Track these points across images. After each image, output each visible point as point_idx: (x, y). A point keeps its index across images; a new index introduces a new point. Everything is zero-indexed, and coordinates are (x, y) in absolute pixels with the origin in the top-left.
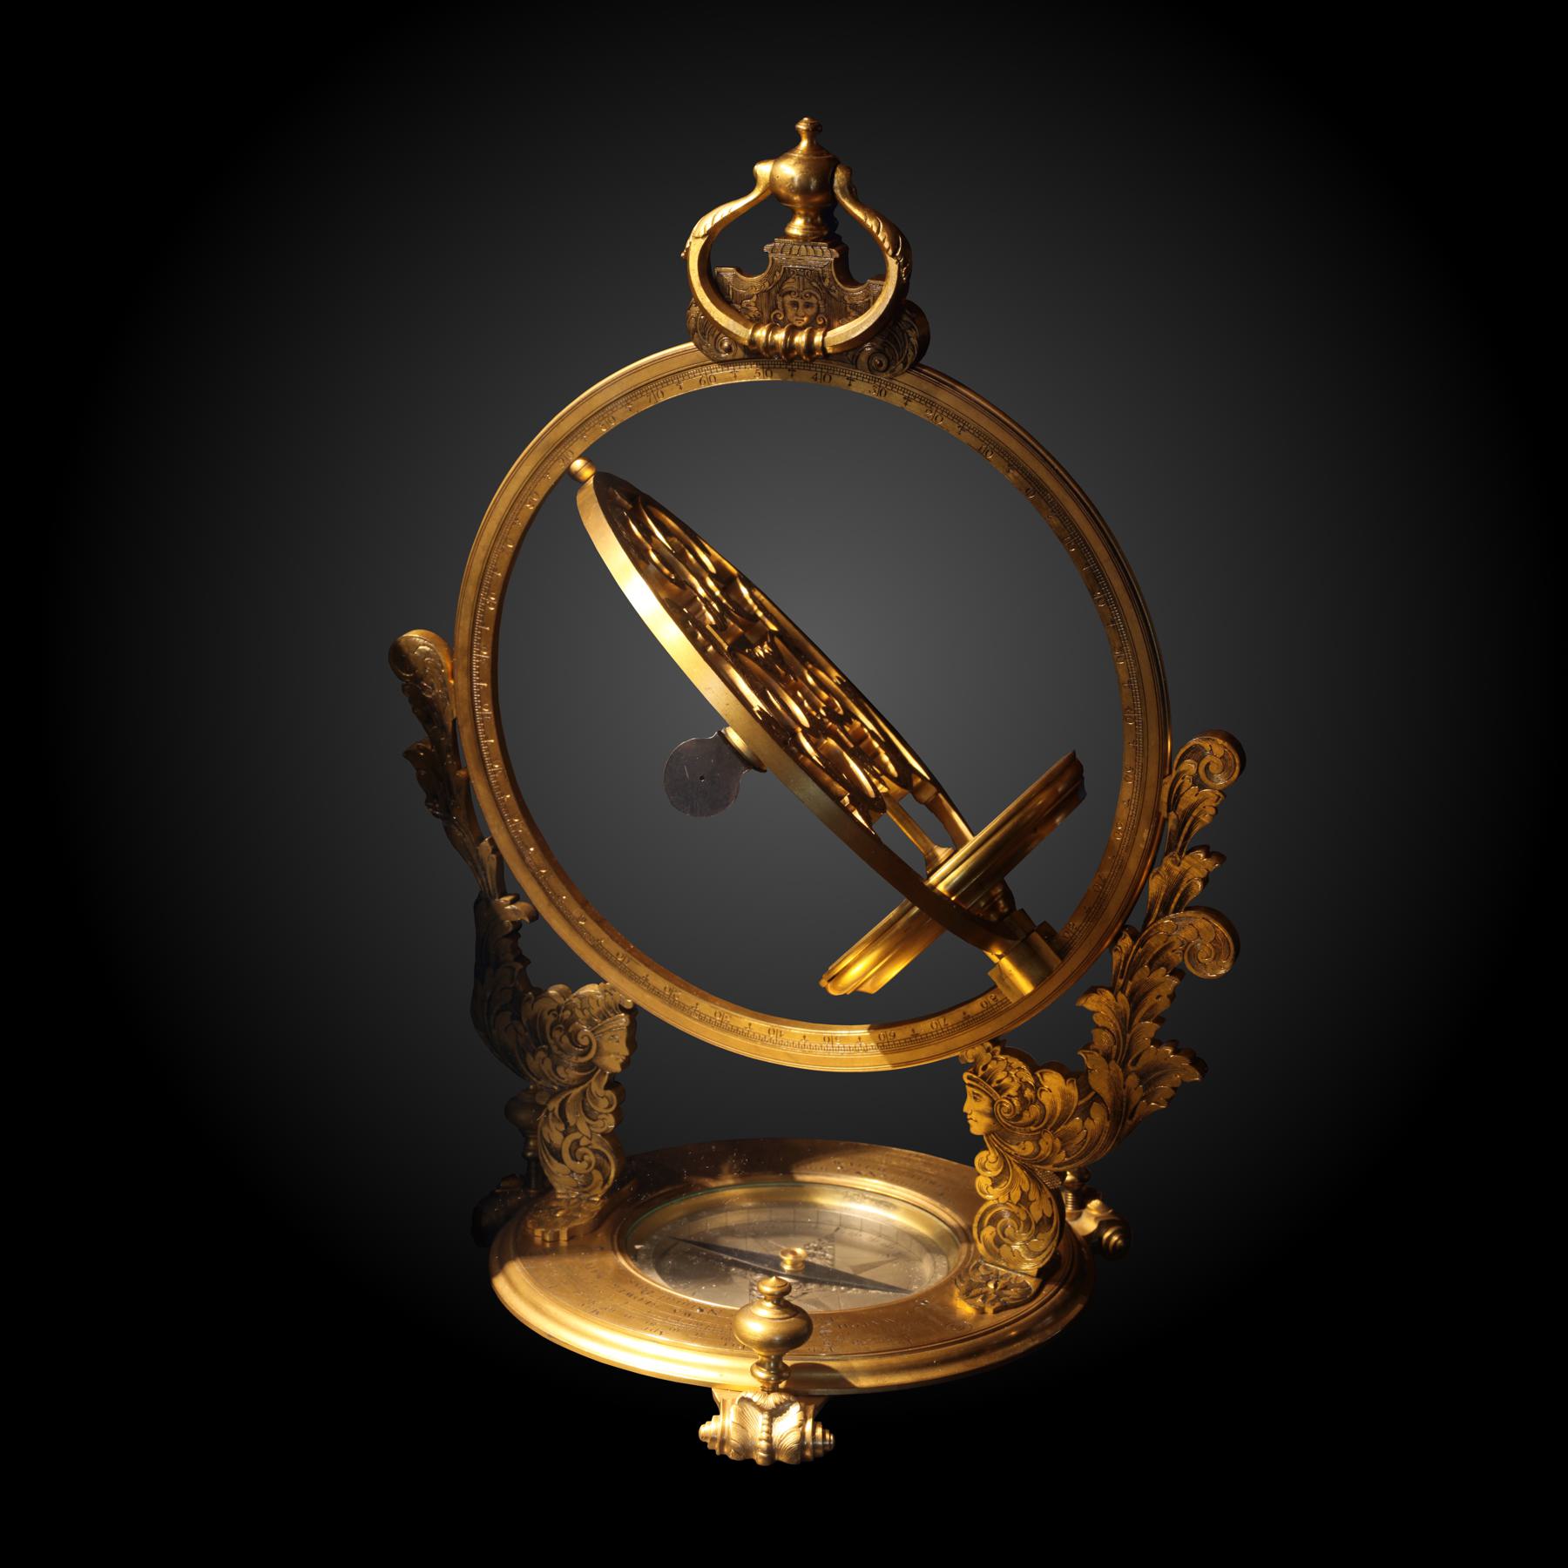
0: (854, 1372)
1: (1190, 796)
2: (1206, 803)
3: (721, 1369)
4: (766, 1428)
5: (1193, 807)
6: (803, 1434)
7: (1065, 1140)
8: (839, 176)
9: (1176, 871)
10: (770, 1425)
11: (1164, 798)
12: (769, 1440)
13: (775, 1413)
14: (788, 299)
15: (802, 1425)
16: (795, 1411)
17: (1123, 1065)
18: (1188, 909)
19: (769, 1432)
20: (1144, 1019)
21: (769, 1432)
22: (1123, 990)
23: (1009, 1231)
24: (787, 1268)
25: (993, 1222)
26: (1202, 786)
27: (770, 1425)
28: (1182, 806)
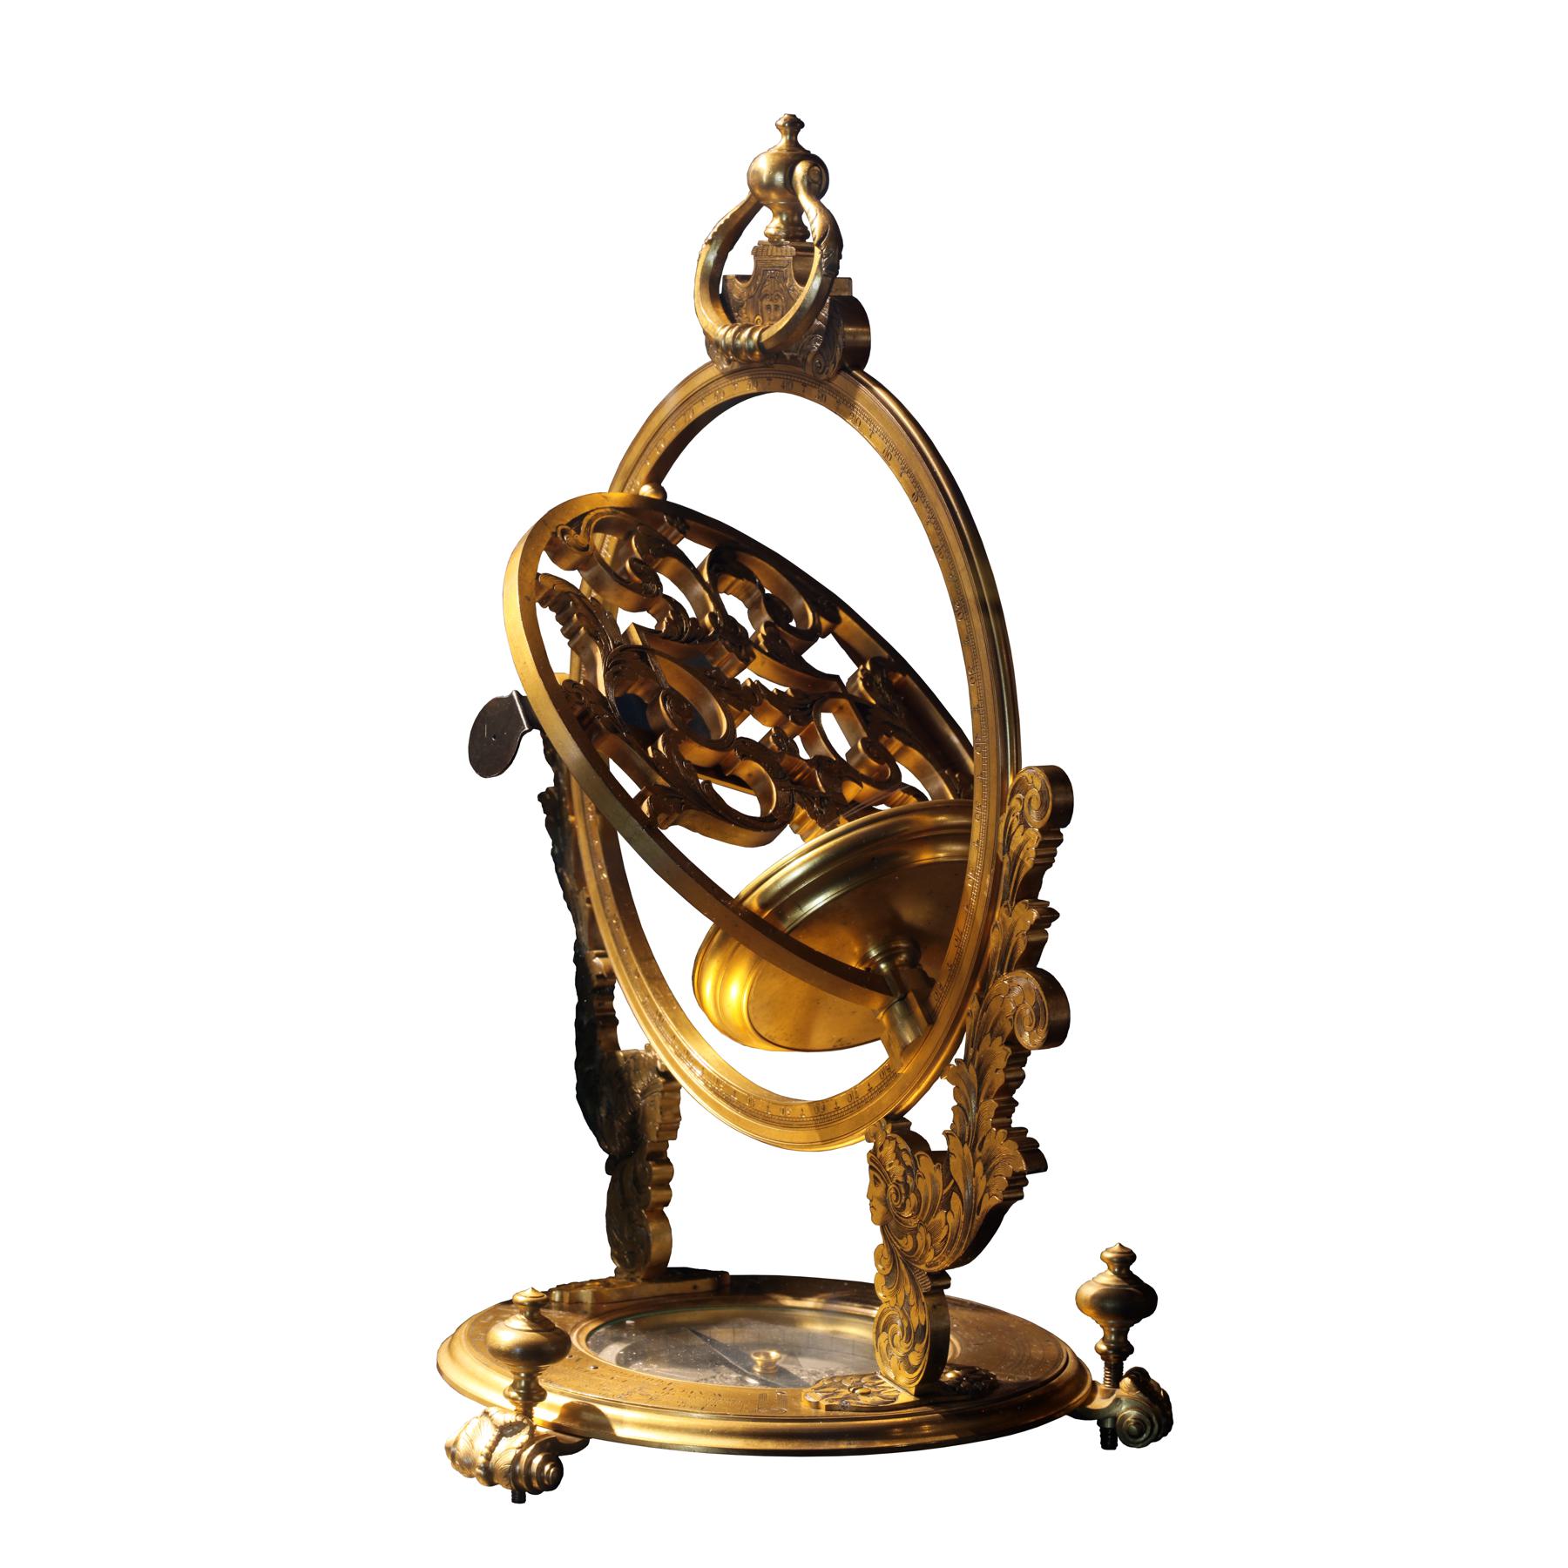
0: (621, 1422)
1: (1018, 839)
2: (1029, 845)
3: (482, 1381)
4: (490, 1444)
5: (1021, 848)
6: (517, 1458)
7: (932, 1233)
8: (801, 170)
9: (1009, 921)
10: (496, 1443)
11: (1001, 840)
12: (488, 1457)
13: (505, 1430)
14: (766, 302)
15: (523, 1448)
16: (523, 1436)
17: (973, 1151)
18: (1017, 967)
19: (492, 1450)
20: (987, 1097)
21: (492, 1450)
22: (972, 1060)
23: (897, 1338)
24: (758, 1370)
25: (885, 1329)
26: (1027, 827)
27: (496, 1443)
28: (1013, 848)
